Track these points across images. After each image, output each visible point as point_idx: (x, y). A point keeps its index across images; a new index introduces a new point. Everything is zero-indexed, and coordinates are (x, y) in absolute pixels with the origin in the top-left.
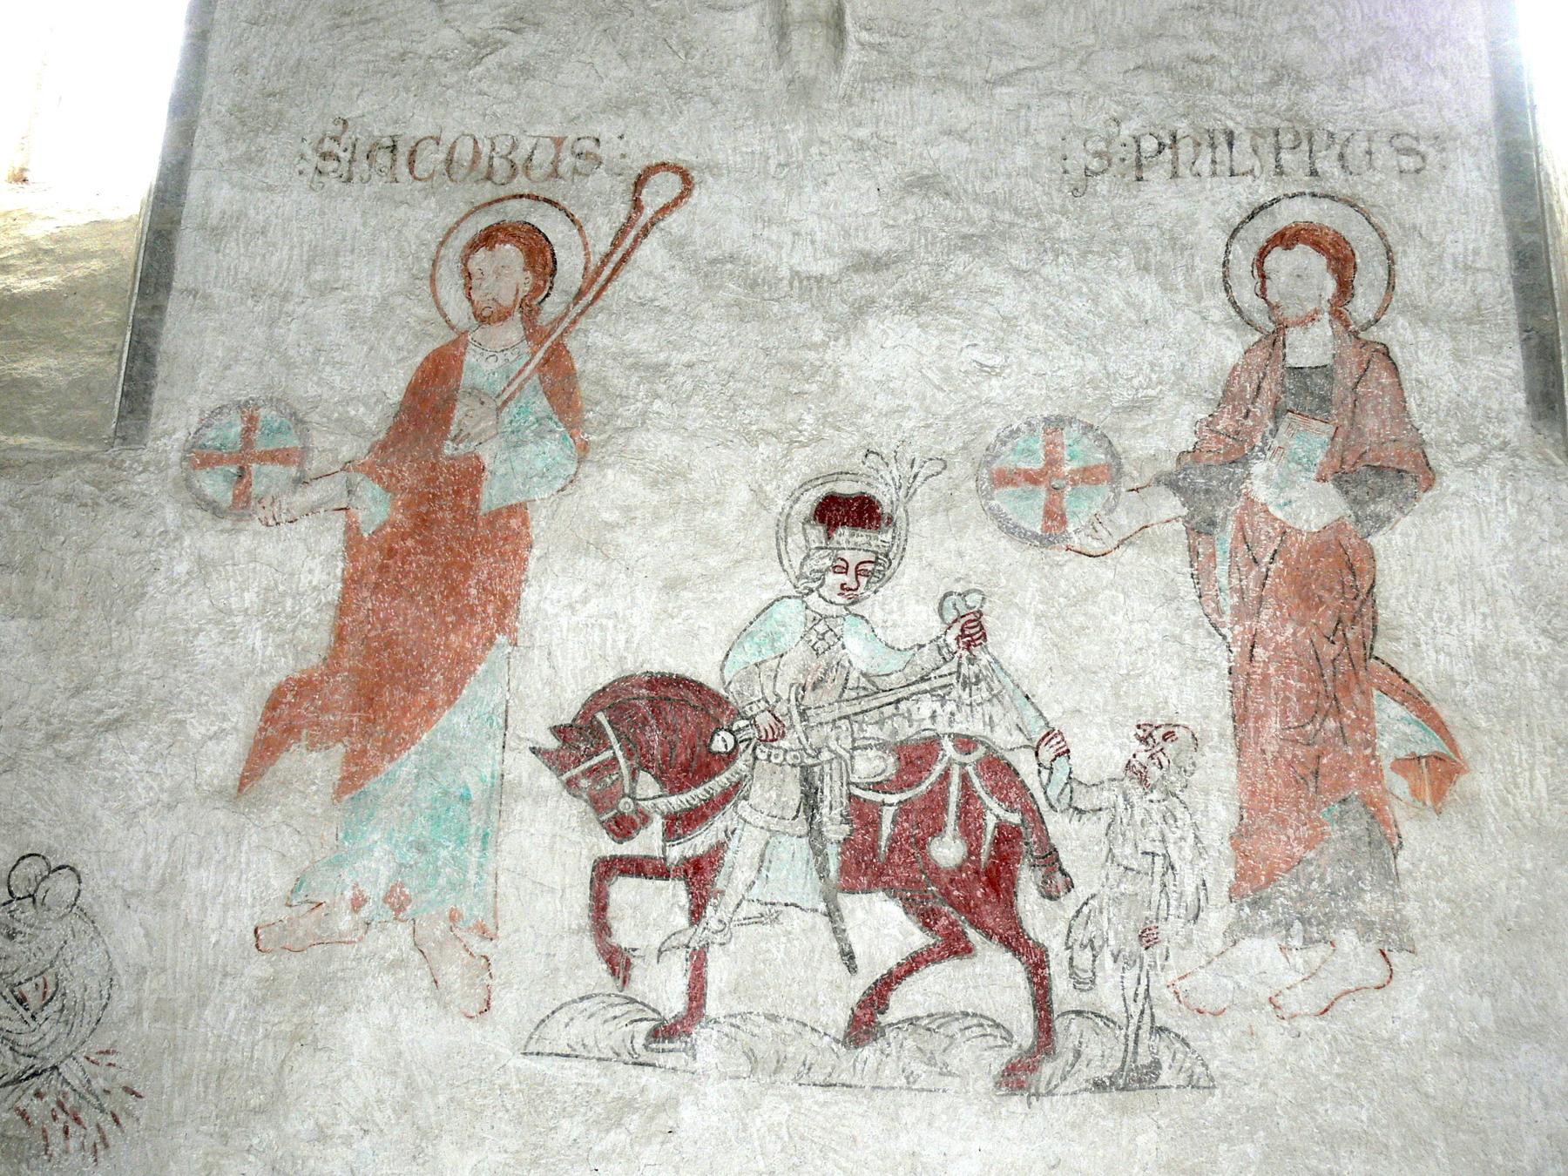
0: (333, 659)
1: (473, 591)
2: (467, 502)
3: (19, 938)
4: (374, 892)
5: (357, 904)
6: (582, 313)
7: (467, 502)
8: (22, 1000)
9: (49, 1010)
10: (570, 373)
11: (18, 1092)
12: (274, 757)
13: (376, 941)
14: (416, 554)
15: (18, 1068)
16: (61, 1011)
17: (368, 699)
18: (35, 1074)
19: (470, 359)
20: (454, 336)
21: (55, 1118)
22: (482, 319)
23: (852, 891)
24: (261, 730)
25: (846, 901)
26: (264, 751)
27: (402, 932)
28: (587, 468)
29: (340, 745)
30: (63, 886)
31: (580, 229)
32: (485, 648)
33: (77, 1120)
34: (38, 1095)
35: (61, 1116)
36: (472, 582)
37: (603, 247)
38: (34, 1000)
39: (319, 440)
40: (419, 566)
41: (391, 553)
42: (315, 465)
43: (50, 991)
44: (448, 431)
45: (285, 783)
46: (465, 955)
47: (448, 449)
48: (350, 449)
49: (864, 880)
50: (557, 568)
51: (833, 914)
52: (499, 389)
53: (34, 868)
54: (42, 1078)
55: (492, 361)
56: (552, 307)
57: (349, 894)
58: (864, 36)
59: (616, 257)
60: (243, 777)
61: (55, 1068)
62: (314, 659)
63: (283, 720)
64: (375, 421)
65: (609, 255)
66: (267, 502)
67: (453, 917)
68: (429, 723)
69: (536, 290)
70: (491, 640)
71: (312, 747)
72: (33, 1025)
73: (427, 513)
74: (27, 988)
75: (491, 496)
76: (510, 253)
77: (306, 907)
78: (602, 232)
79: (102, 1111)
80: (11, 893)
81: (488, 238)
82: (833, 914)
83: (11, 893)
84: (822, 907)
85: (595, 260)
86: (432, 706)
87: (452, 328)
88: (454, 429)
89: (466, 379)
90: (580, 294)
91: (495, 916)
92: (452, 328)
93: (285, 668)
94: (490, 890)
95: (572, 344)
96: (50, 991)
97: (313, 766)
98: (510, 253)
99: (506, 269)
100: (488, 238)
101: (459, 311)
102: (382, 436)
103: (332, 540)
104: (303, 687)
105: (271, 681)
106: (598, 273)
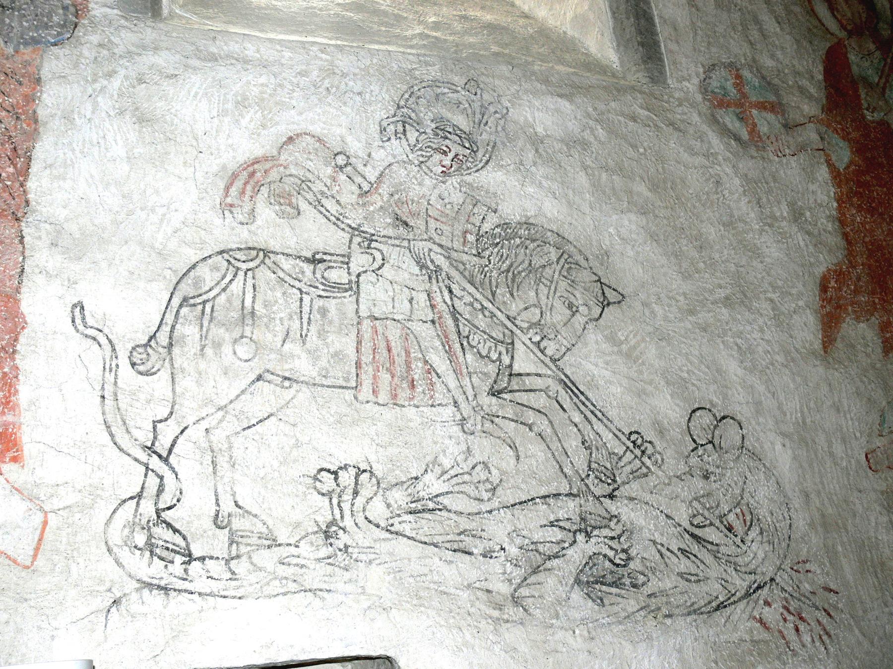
0: (850, 254)
3: (712, 478)
8: (730, 529)
9: (753, 534)
11: (752, 604)
15: (745, 584)
16: (761, 533)
18: (759, 587)
20: (836, 40)
21: (785, 620)
24: (822, 307)
29: (873, 318)
33: (801, 618)
34: (767, 603)
35: (790, 618)
40: (878, 194)
43: (748, 518)
54: (766, 589)
60: (824, 343)
61: (772, 580)
72: (744, 548)
74: (731, 517)
79: (817, 608)
80: (694, 441)
83: (694, 441)
88: (865, 105)
96: (748, 518)
104: (839, 274)
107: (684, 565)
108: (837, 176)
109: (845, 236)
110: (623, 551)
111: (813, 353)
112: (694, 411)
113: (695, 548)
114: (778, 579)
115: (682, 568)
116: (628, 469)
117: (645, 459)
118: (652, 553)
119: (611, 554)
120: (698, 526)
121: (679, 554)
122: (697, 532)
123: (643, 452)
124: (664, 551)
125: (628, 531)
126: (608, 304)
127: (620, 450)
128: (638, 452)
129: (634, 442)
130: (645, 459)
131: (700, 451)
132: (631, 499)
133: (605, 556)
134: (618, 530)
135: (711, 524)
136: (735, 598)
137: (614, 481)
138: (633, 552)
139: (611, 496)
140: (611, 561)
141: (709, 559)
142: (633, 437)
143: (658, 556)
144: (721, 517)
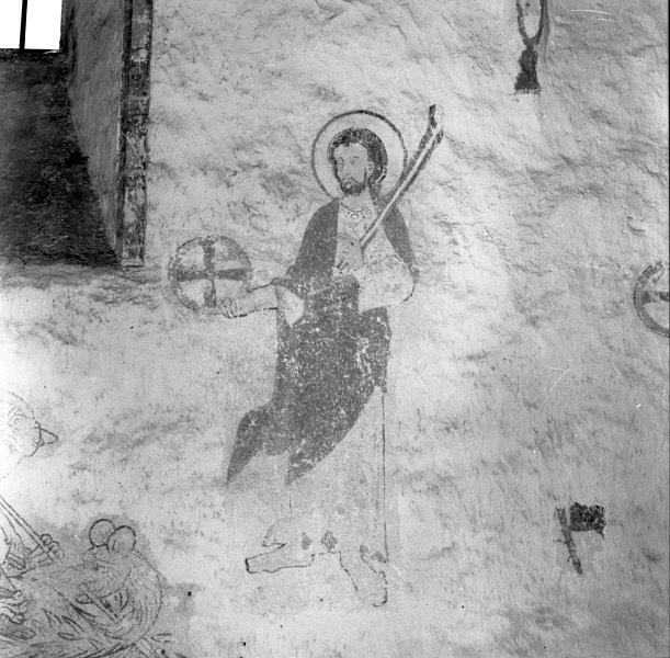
0: (278, 400)
1: (358, 360)
2: (350, 305)
3: (101, 570)
4: (316, 535)
5: (306, 543)
6: (406, 189)
7: (350, 305)
8: (108, 606)
9: (125, 612)
10: (403, 229)
12: (247, 458)
13: (319, 564)
14: (322, 337)
16: (133, 611)
17: (301, 422)
18: (122, 649)
19: (342, 215)
20: (329, 200)
22: (347, 192)
23: (579, 530)
24: (238, 442)
25: (575, 535)
26: (241, 455)
27: (335, 559)
28: (418, 286)
29: (286, 452)
30: (125, 537)
31: (400, 135)
32: (368, 395)
36: (358, 354)
37: (416, 147)
38: (114, 604)
39: (257, 265)
40: (324, 344)
41: (306, 335)
42: (256, 280)
43: (124, 600)
44: (334, 261)
45: (255, 474)
46: (371, 571)
47: (336, 272)
48: (278, 271)
49: (584, 524)
50: (407, 347)
51: (569, 542)
52: (361, 235)
53: (105, 528)
55: (357, 218)
56: (388, 183)
57: (301, 539)
58: (558, 19)
59: (423, 155)
61: (133, 644)
62: (267, 400)
63: (250, 437)
64: (290, 253)
65: (419, 153)
66: (227, 302)
67: (362, 550)
68: (339, 439)
69: (377, 174)
70: (372, 388)
71: (269, 453)
72: (116, 620)
73: (328, 312)
74: (110, 599)
75: (365, 302)
76: (358, 148)
77: (276, 546)
78: (414, 139)
80: (92, 542)
81: (345, 139)
82: (569, 542)
83: (92, 542)
84: (563, 539)
85: (411, 156)
86: (340, 428)
87: (328, 195)
88: (337, 262)
89: (340, 228)
90: (403, 177)
91: (386, 548)
92: (328, 195)
93: (249, 406)
94: (382, 534)
95: (403, 209)
96: (124, 600)
97: (270, 464)
98: (358, 148)
99: (356, 159)
100: (345, 139)
101: (333, 188)
102: (293, 263)
103: (271, 328)
104: (262, 416)
105: (242, 413)
106: (413, 163)
107: (67, 628)
108: (285, 332)
109: (280, 384)
110: (21, 614)
111: (216, 480)
112: (97, 522)
113: (75, 617)
114: (139, 645)
115: (62, 630)
116: (37, 559)
117: (51, 554)
118: (41, 617)
119: (11, 615)
120: (82, 603)
121: (62, 620)
122: (79, 606)
123: (50, 549)
124: (52, 616)
125: (29, 601)
126: (43, 444)
127: (33, 547)
128: (46, 549)
129: (44, 542)
130: (51, 554)
131: (96, 550)
132: (34, 580)
133: (7, 616)
134: (20, 600)
135: (92, 602)
136: (101, 654)
137: (24, 567)
138: (27, 616)
139: (19, 577)
140: (10, 620)
141: (86, 625)
142: (45, 538)
143: (46, 620)
144: (101, 598)
